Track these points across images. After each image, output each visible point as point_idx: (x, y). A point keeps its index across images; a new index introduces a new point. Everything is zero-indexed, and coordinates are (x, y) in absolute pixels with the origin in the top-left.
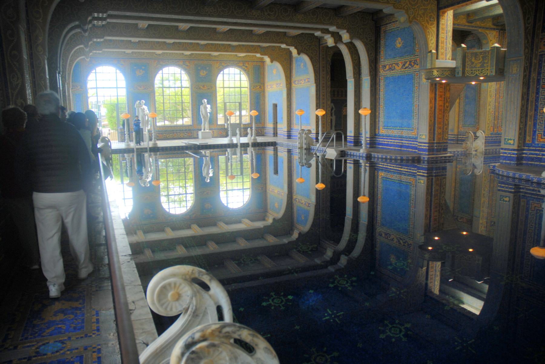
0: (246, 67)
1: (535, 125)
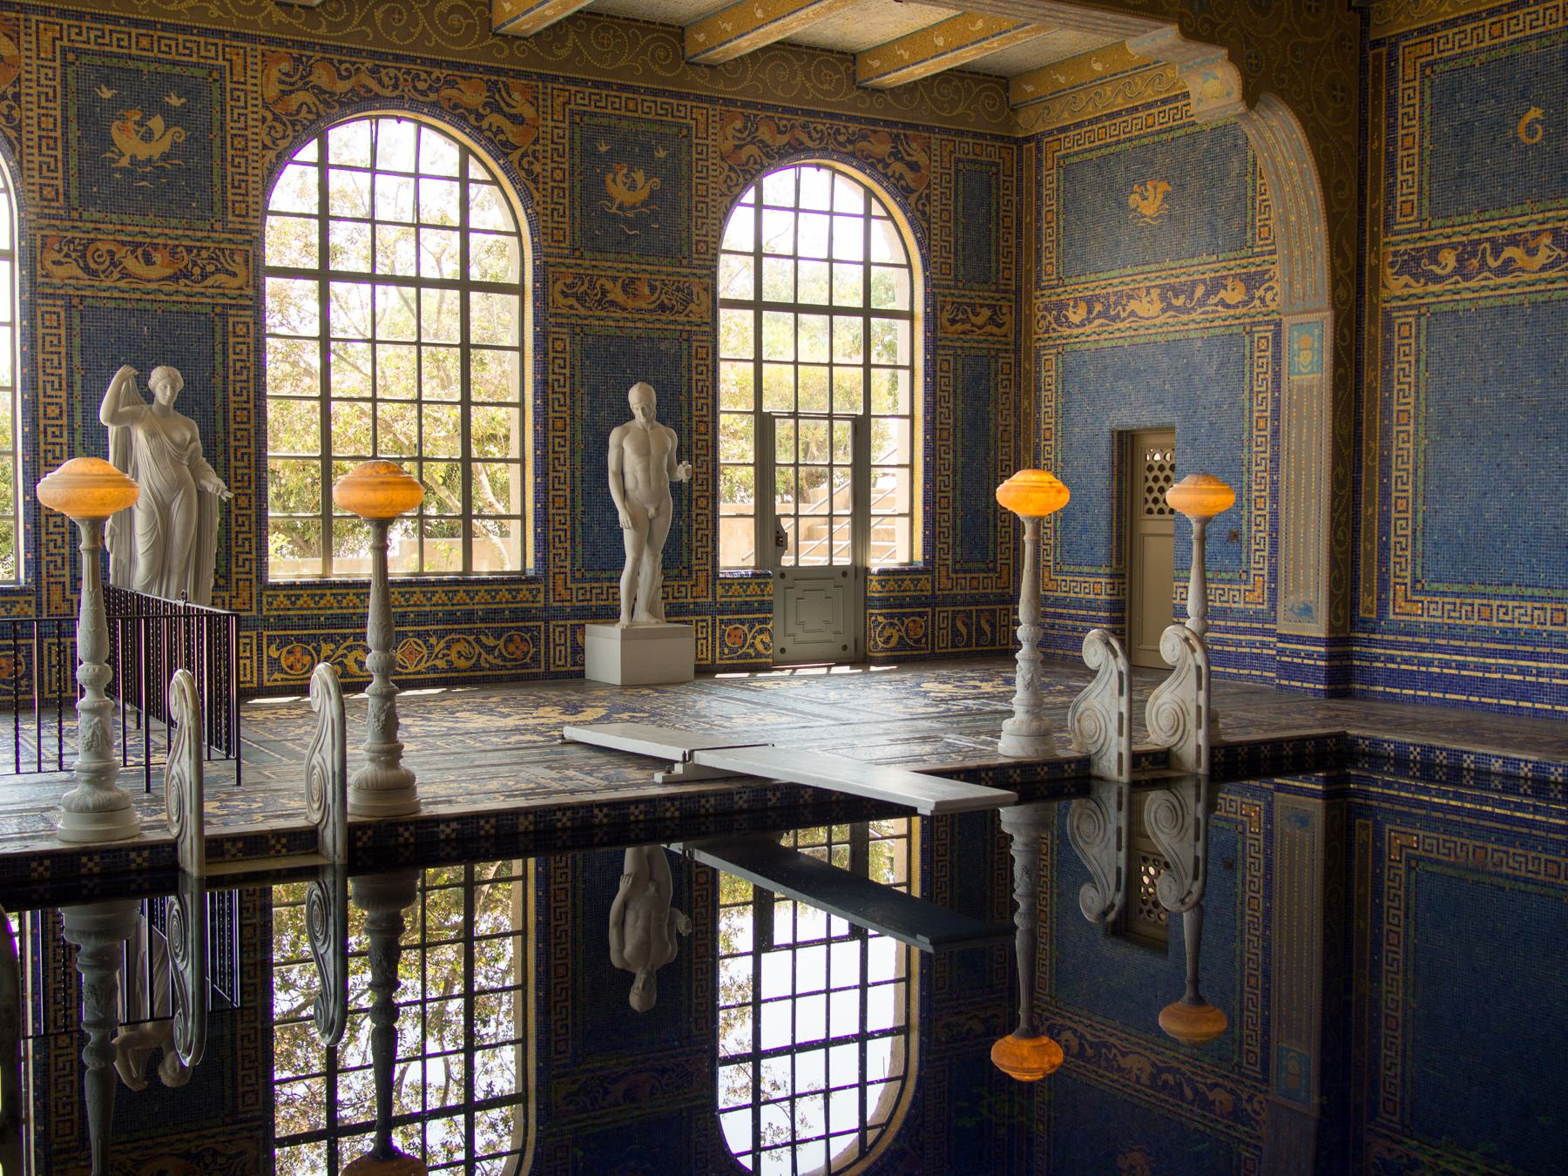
0: (914, 167)
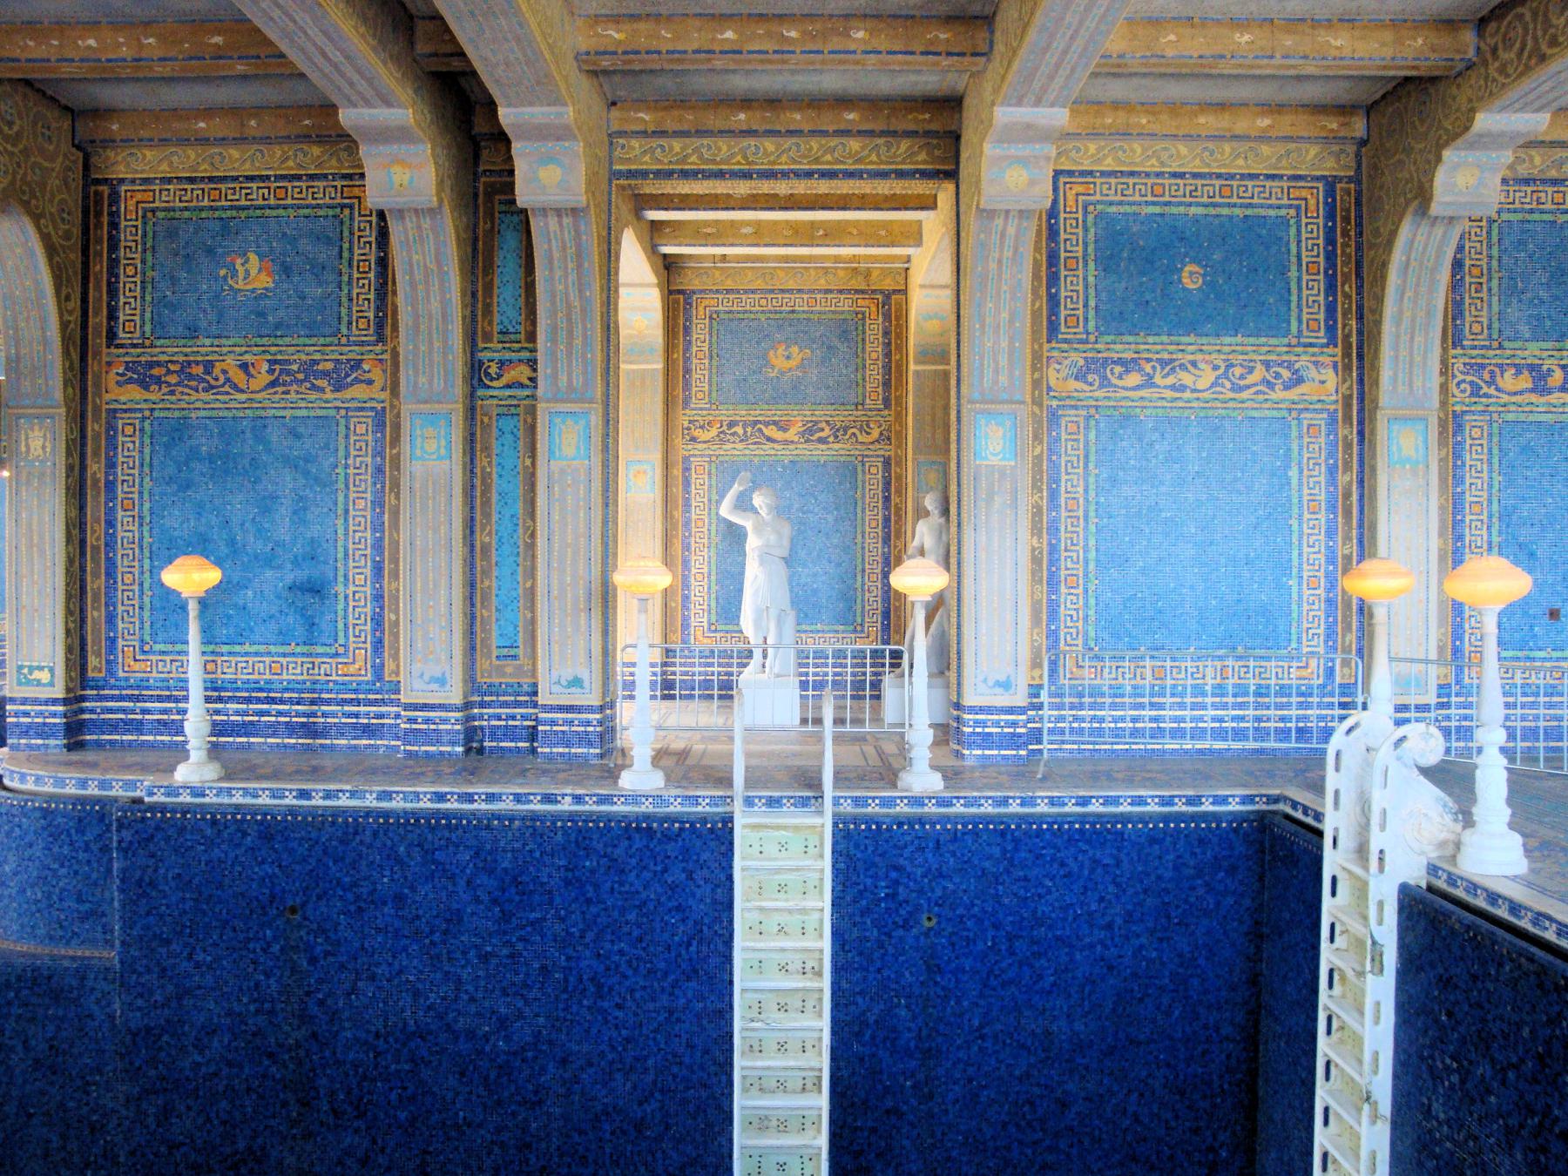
1: (111, 619)
